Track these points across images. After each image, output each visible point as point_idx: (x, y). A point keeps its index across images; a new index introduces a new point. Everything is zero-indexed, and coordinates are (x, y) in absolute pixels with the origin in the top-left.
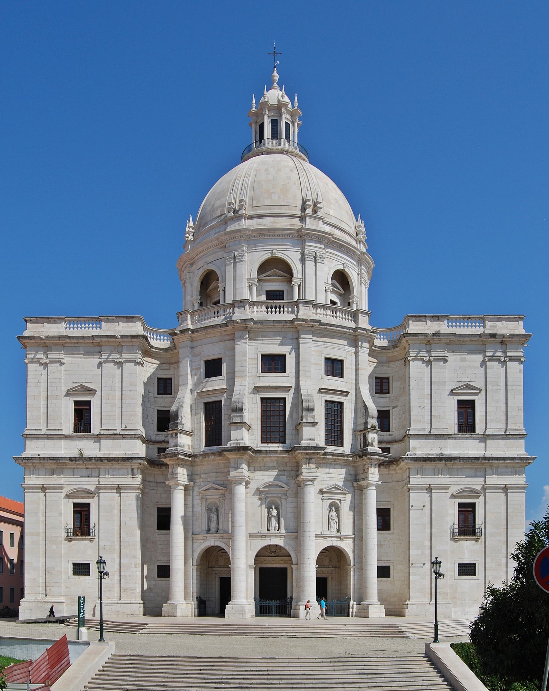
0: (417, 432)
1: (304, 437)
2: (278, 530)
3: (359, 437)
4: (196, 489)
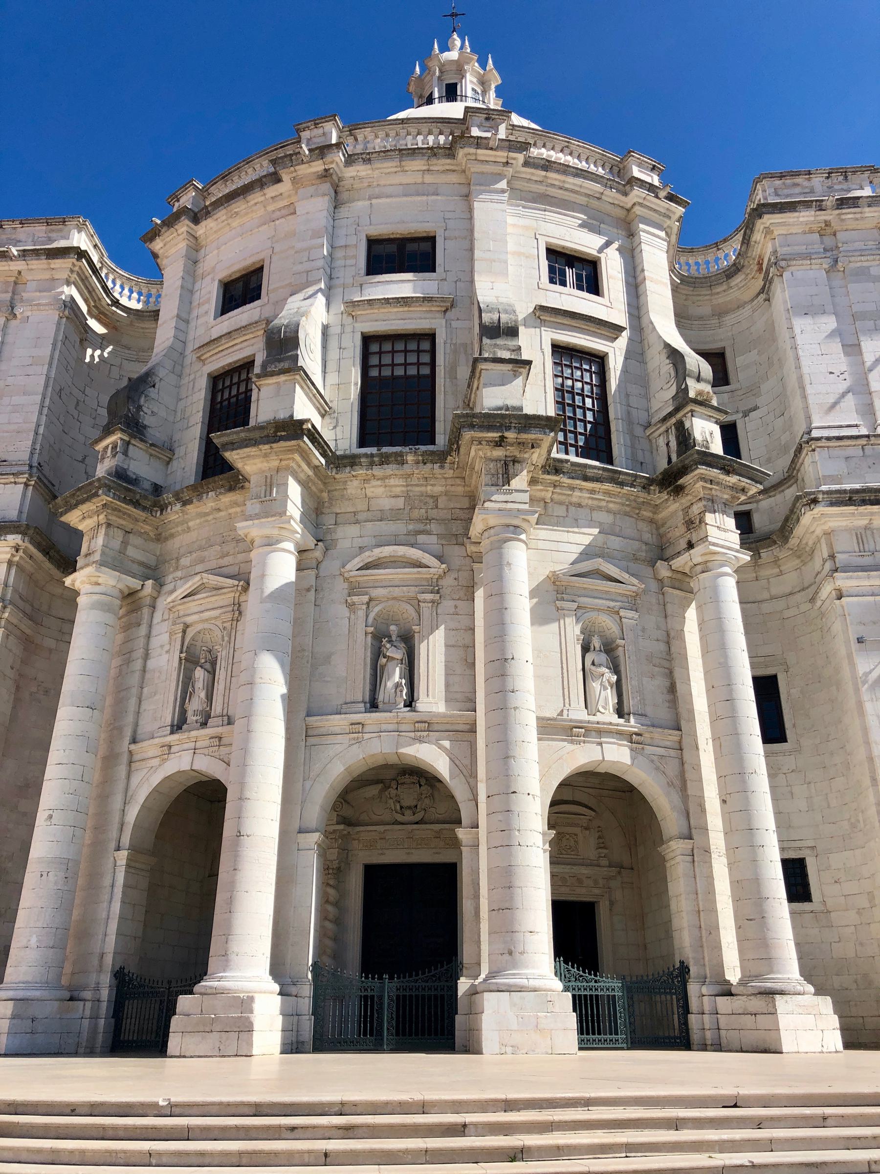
3: (662, 442)
4: (164, 602)
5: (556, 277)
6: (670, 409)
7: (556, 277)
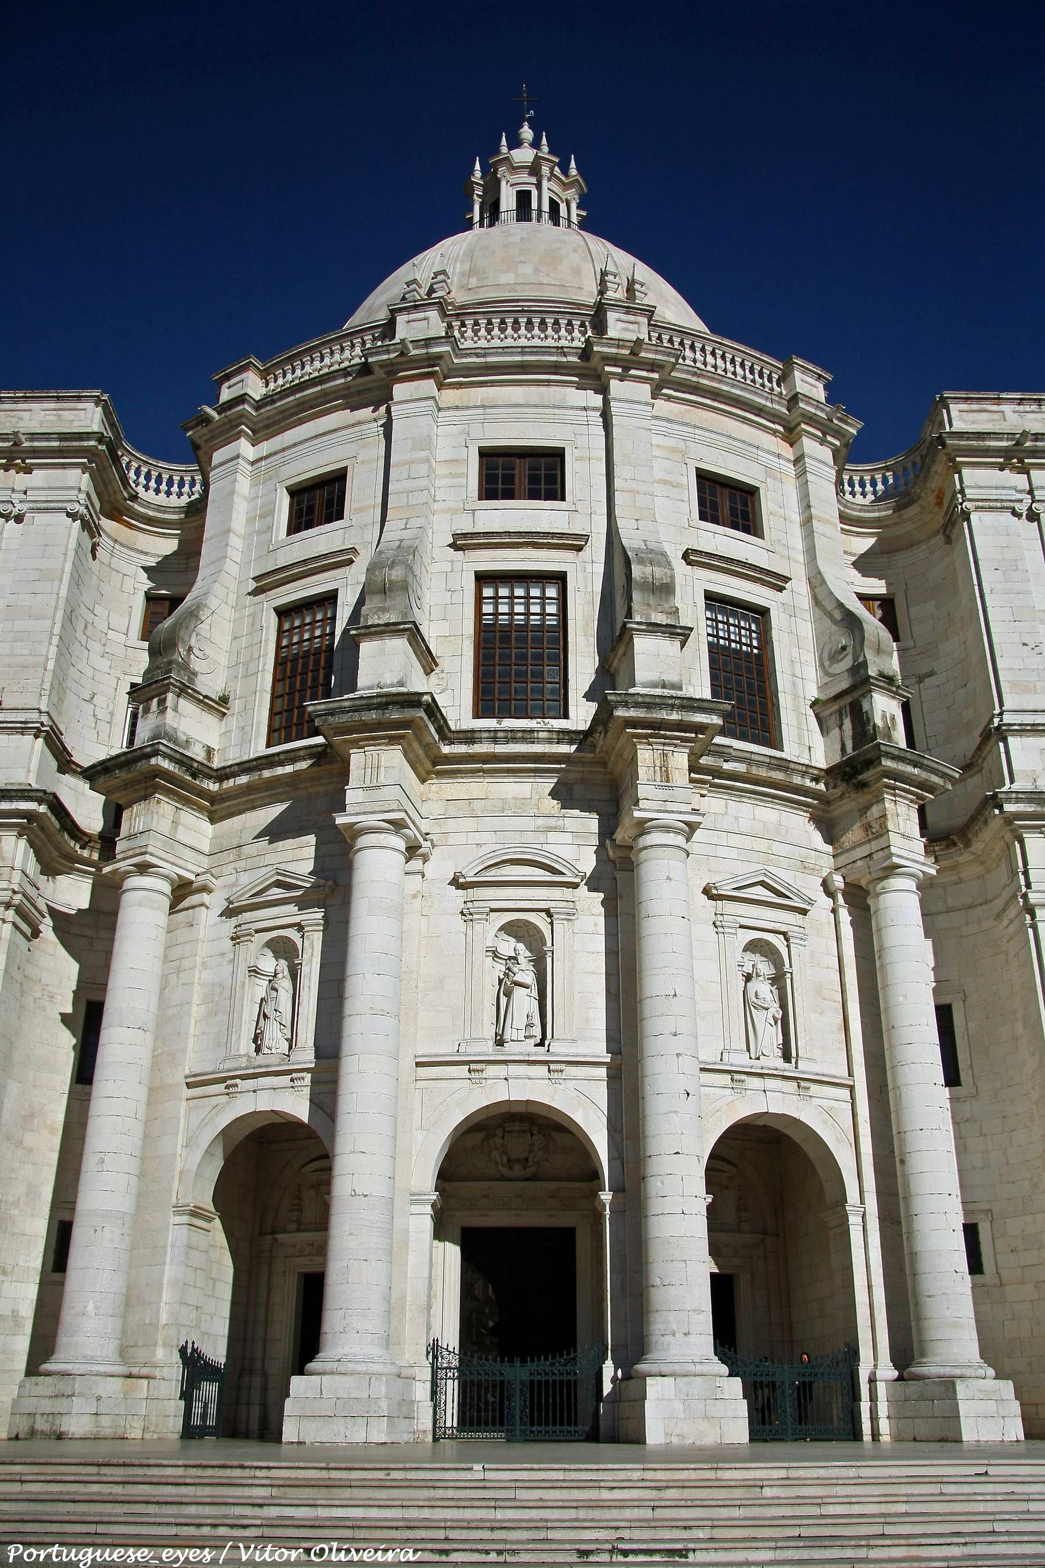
0: (1029, 719)
1: (640, 675)
2: (541, 1044)
5: (708, 512)
6: (845, 685)
7: (708, 512)
